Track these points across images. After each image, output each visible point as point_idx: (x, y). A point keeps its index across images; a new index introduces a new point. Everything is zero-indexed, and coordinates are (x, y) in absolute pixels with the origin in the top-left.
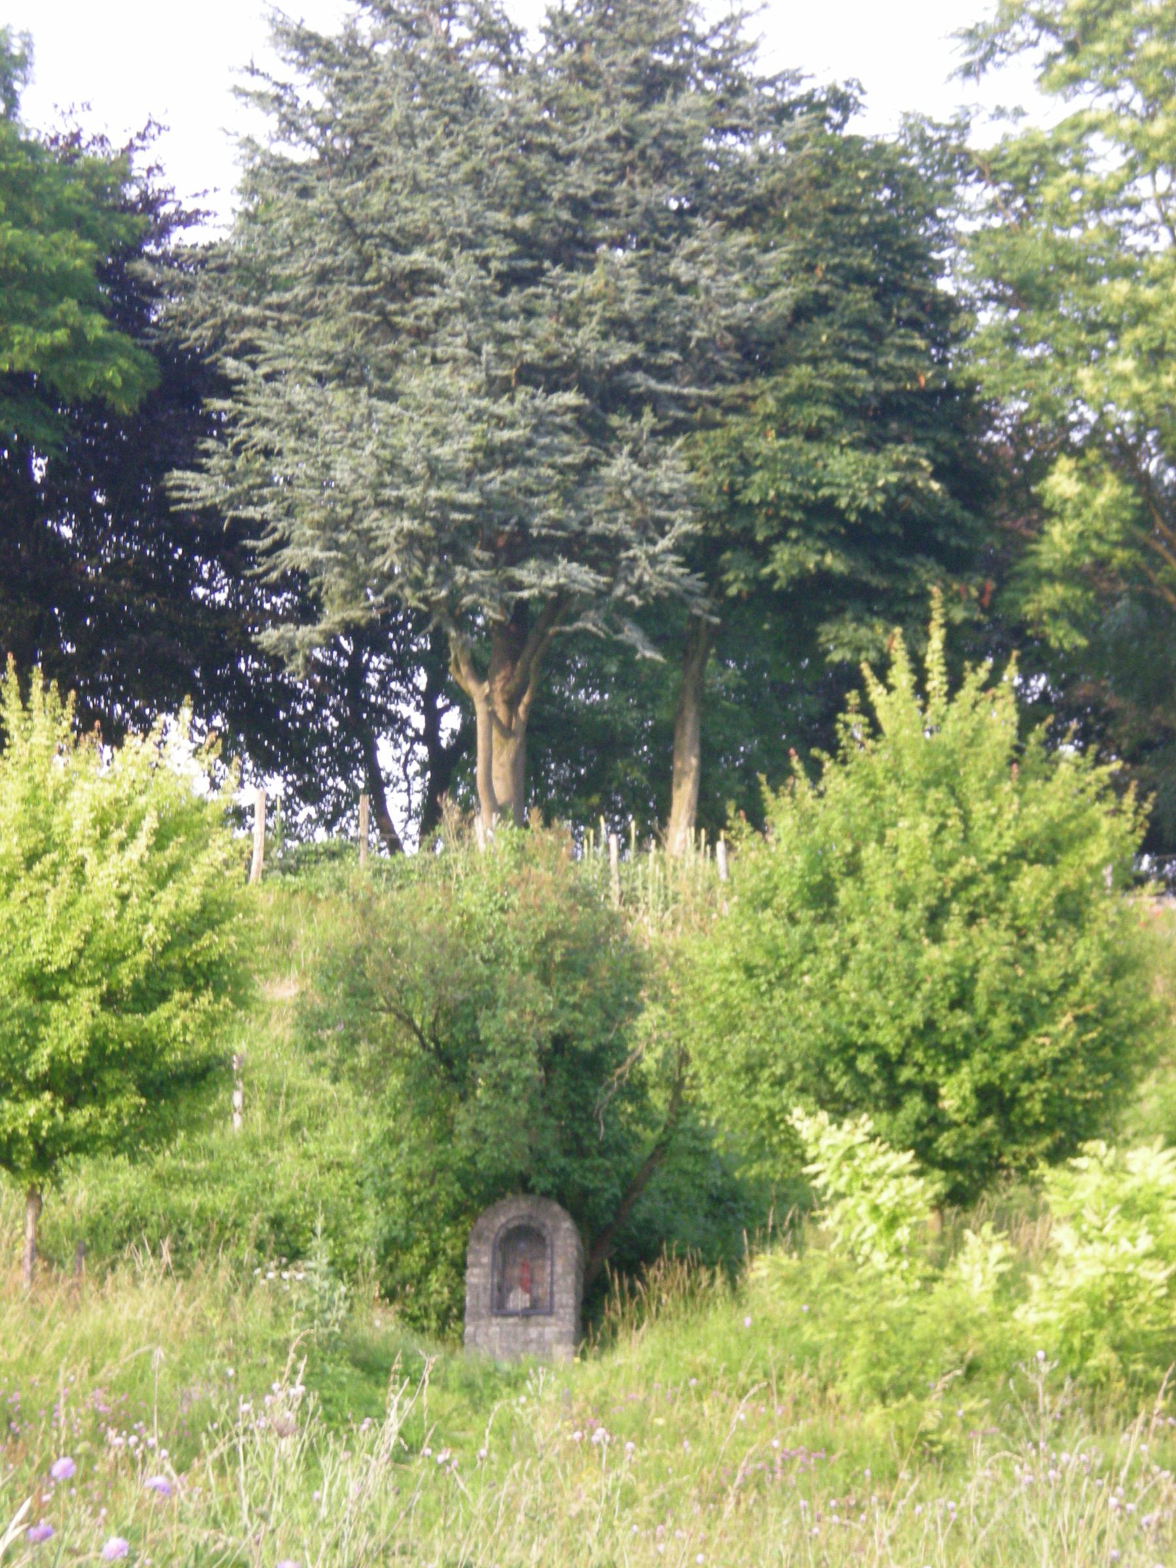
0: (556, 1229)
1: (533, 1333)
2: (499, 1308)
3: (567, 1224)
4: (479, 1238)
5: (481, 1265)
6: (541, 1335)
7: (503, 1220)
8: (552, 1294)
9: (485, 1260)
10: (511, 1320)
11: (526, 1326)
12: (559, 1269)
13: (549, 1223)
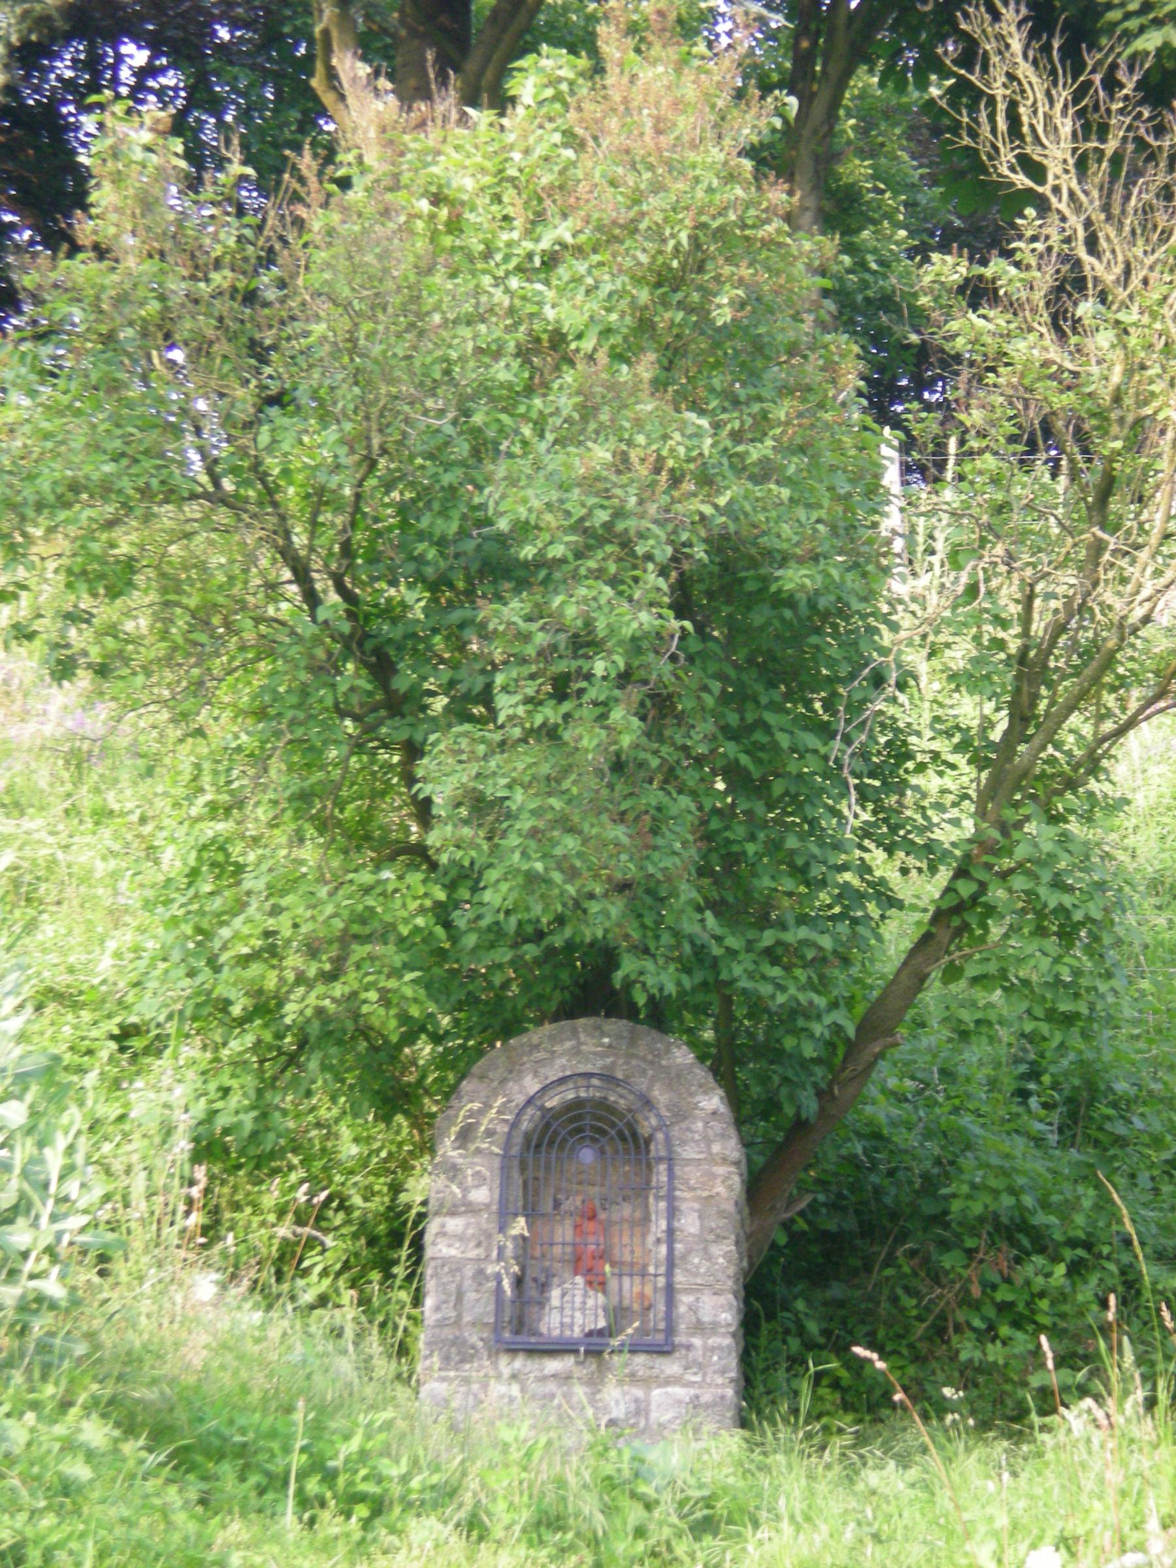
5: (471, 1209)
11: (595, 1383)
12: (689, 1223)
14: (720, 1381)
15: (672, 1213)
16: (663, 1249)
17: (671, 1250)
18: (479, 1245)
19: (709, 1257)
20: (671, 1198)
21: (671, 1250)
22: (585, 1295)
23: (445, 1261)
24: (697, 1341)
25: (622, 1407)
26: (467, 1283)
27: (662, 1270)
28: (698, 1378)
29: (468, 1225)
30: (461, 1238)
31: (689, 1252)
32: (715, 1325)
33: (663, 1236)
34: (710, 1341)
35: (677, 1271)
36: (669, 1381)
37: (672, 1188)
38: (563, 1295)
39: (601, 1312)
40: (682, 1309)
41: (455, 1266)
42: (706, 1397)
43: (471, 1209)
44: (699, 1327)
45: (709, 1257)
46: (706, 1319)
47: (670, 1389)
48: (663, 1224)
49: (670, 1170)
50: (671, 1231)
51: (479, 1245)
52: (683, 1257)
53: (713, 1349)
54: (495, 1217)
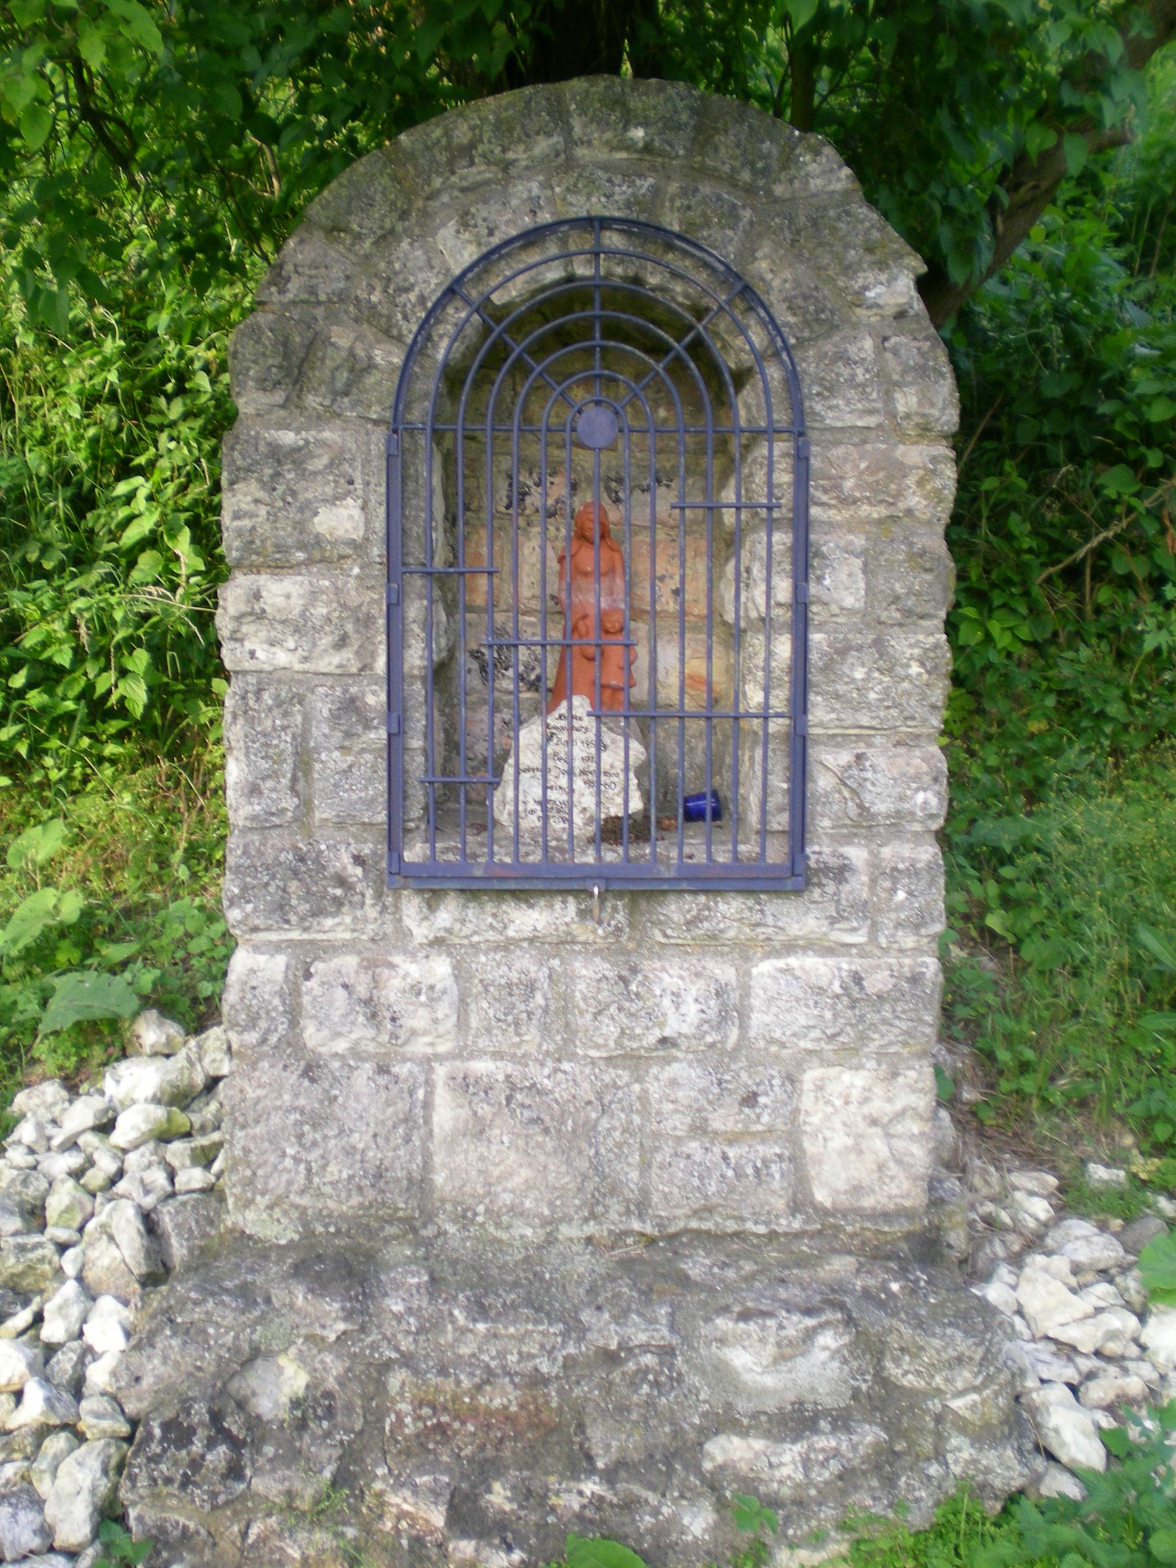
0: (826, 318)
1: (679, 993)
2: (442, 817)
3: (895, 287)
4: (294, 369)
5: (320, 554)
6: (731, 1008)
7: (457, 250)
8: (799, 745)
9: (343, 520)
10: (528, 919)
12: (842, 586)
13: (773, 273)
14: (909, 941)
15: (804, 562)
16: (784, 648)
17: (801, 648)
18: (342, 642)
19: (888, 664)
20: (801, 525)
21: (801, 648)
22: (600, 746)
23: (265, 679)
24: (857, 854)
25: (691, 1009)
26: (320, 731)
27: (780, 700)
28: (860, 938)
29: (314, 595)
30: (300, 627)
31: (843, 651)
32: (897, 823)
33: (782, 615)
34: (886, 852)
35: (814, 698)
36: (790, 948)
37: (803, 500)
38: (548, 738)
39: (634, 781)
40: (822, 782)
41: (292, 692)
42: (878, 982)
43: (320, 554)
44: (864, 824)
45: (888, 664)
46: (881, 807)
47: (793, 961)
48: (783, 589)
49: (801, 461)
50: (801, 608)
51: (342, 642)
52: (827, 668)
53: (895, 874)
54: (378, 571)
